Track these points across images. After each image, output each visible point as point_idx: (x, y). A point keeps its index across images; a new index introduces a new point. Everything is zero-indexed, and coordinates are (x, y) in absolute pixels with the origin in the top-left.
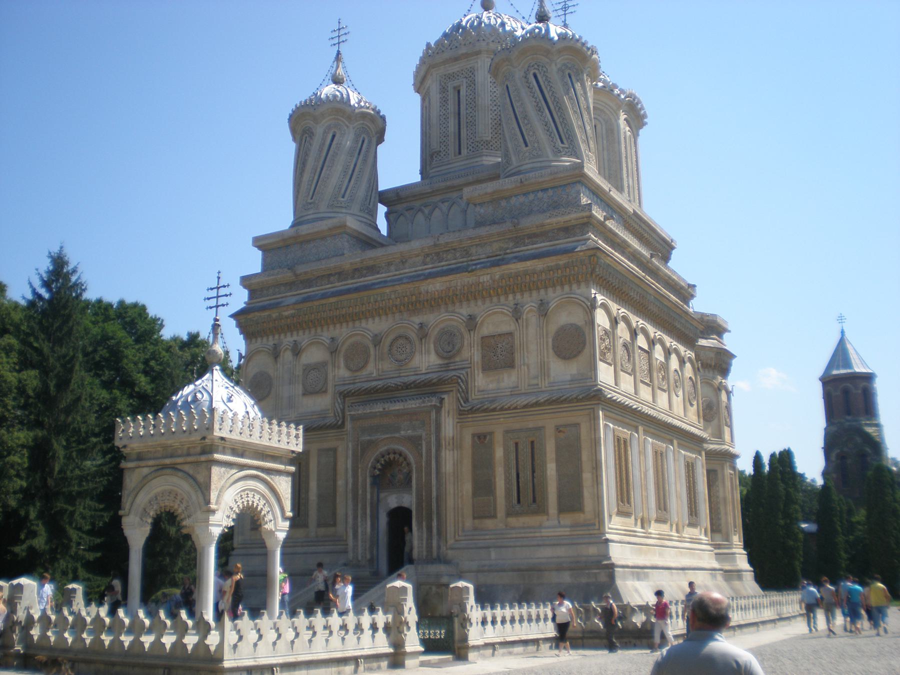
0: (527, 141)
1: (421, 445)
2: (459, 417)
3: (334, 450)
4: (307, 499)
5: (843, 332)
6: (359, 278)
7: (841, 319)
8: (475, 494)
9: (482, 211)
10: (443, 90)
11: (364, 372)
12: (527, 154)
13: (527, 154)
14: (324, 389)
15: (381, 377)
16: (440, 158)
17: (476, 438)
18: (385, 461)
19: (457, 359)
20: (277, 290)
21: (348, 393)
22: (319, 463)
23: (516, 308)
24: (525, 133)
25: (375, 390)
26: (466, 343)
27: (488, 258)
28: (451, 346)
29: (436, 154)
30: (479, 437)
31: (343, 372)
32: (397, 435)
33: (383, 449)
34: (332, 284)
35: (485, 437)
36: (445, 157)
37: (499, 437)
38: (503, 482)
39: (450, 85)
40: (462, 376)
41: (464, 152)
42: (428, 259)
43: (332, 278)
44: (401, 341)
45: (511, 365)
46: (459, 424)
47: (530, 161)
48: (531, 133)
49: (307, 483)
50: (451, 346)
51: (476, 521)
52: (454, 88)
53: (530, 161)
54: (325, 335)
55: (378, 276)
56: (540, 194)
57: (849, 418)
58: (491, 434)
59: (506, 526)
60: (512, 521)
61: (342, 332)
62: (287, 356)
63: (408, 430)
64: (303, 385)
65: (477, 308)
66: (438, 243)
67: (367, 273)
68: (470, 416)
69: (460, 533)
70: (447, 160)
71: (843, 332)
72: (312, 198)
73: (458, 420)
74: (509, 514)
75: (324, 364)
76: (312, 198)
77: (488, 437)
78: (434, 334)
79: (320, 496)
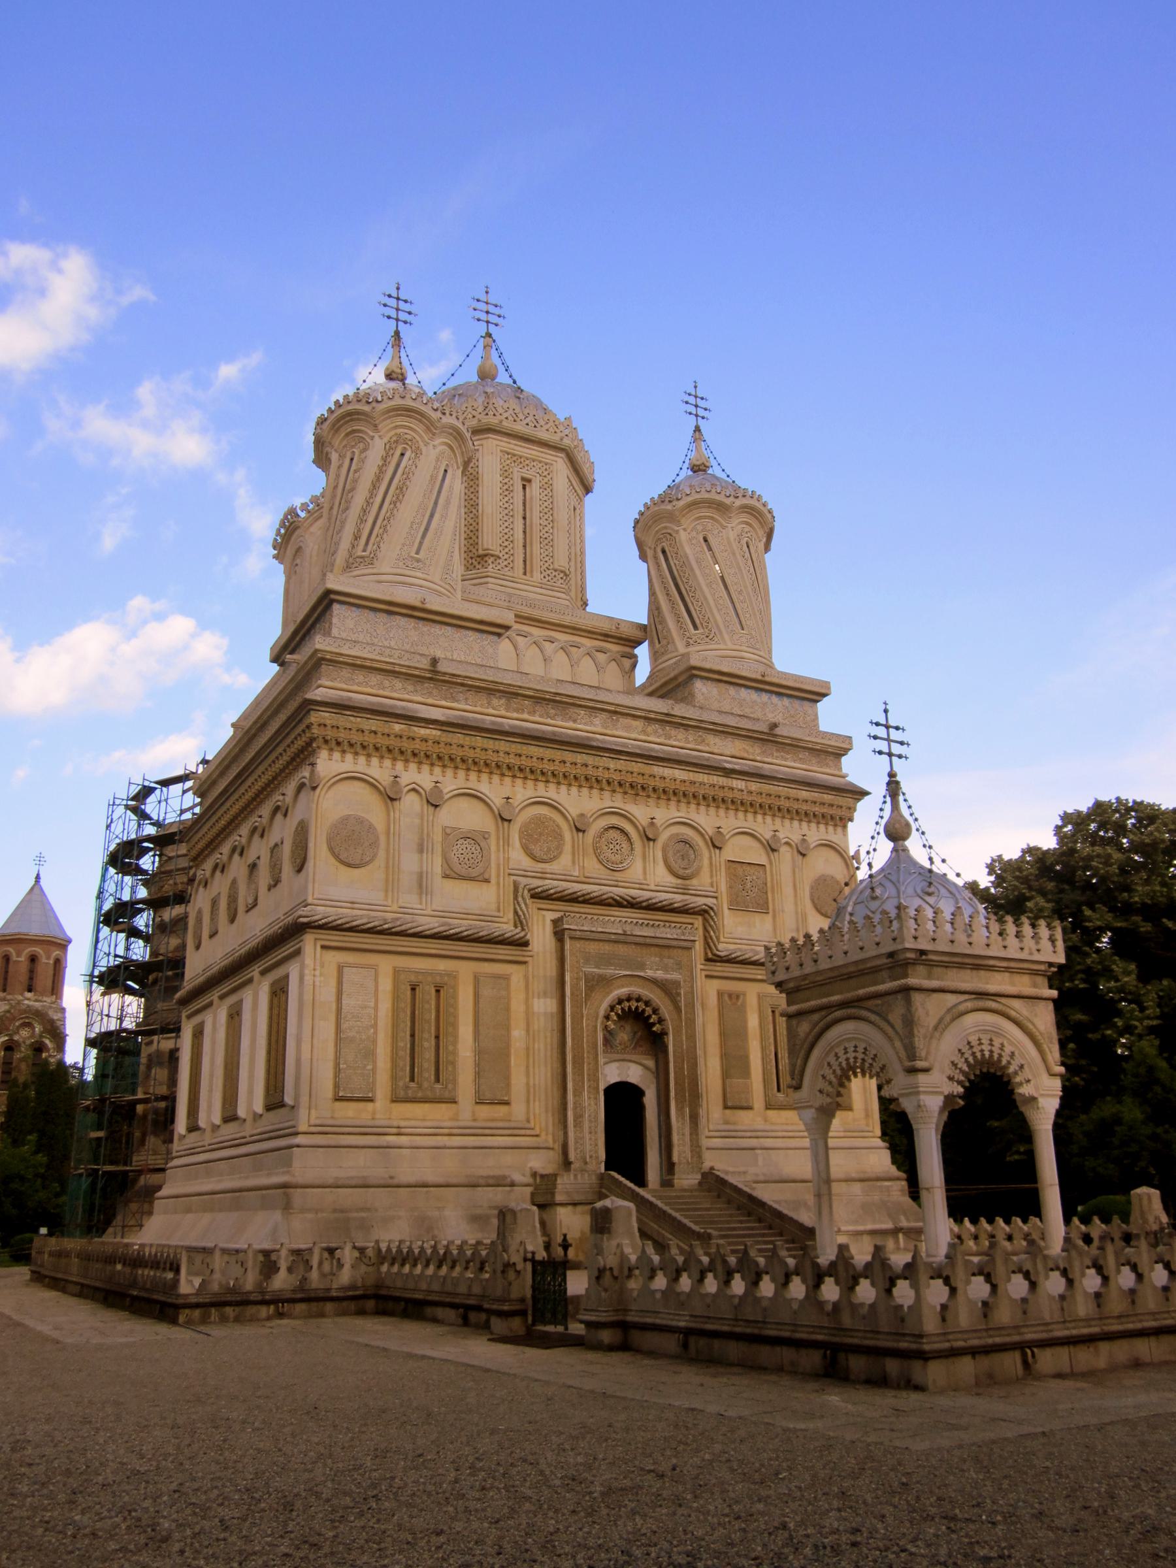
0: (744, 623)
1: (679, 994)
2: (703, 962)
3: (506, 978)
4: (455, 1053)
5: (38, 877)
6: (541, 716)
7: (40, 860)
8: (726, 1075)
9: (704, 690)
10: (506, 473)
11: (554, 867)
12: (744, 640)
13: (744, 640)
14: (486, 876)
15: (587, 880)
16: (499, 567)
17: (726, 998)
18: (622, 1009)
19: (694, 882)
20: (387, 683)
21: (542, 892)
22: (477, 996)
23: (775, 836)
24: (740, 612)
25: (587, 897)
26: (706, 862)
27: (732, 757)
28: (686, 861)
29: (492, 559)
30: (730, 996)
31: (518, 857)
32: (642, 974)
33: (623, 991)
34: (494, 709)
35: (738, 997)
36: (507, 569)
37: (752, 1001)
38: (759, 1062)
39: (517, 473)
40: (715, 908)
41: (537, 576)
42: (650, 729)
43: (495, 702)
44: (612, 834)
45: (762, 907)
46: (704, 973)
47: (751, 650)
48: (748, 616)
49: (455, 1025)
50: (686, 861)
51: (728, 1112)
52: (523, 479)
53: (751, 650)
54: (494, 789)
55: (570, 724)
56: (775, 699)
57: (29, 995)
58: (744, 995)
59: (766, 1121)
60: (771, 1113)
61: (522, 792)
62: (411, 803)
63: (657, 970)
64: (446, 859)
65: (730, 822)
66: (673, 713)
67: (556, 715)
68: (719, 964)
69: (711, 1127)
70: (509, 574)
71: (38, 877)
72: (417, 553)
73: (702, 967)
74: (769, 1107)
75: (485, 836)
76: (417, 553)
77: (742, 997)
78: (664, 837)
79: (479, 1052)
